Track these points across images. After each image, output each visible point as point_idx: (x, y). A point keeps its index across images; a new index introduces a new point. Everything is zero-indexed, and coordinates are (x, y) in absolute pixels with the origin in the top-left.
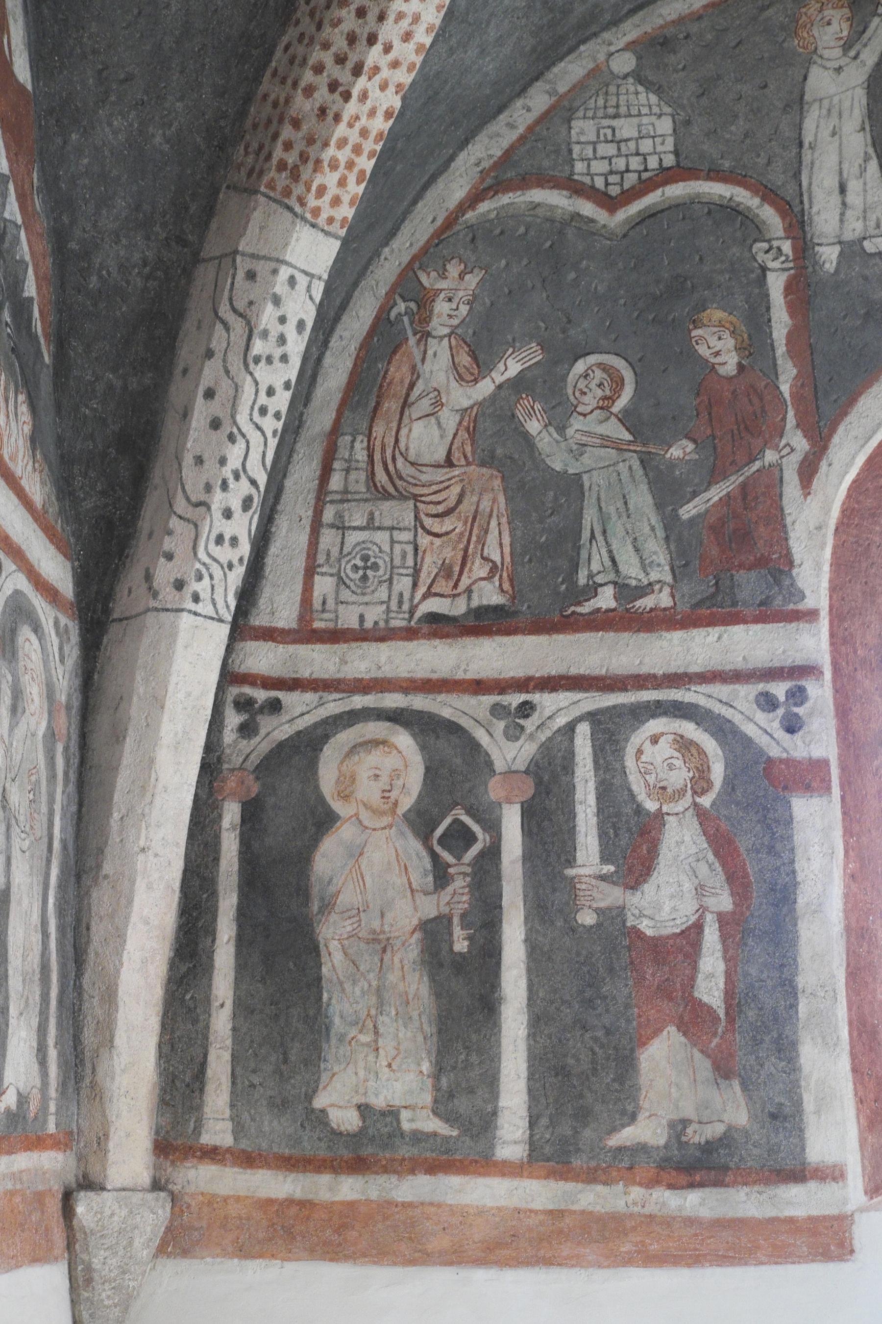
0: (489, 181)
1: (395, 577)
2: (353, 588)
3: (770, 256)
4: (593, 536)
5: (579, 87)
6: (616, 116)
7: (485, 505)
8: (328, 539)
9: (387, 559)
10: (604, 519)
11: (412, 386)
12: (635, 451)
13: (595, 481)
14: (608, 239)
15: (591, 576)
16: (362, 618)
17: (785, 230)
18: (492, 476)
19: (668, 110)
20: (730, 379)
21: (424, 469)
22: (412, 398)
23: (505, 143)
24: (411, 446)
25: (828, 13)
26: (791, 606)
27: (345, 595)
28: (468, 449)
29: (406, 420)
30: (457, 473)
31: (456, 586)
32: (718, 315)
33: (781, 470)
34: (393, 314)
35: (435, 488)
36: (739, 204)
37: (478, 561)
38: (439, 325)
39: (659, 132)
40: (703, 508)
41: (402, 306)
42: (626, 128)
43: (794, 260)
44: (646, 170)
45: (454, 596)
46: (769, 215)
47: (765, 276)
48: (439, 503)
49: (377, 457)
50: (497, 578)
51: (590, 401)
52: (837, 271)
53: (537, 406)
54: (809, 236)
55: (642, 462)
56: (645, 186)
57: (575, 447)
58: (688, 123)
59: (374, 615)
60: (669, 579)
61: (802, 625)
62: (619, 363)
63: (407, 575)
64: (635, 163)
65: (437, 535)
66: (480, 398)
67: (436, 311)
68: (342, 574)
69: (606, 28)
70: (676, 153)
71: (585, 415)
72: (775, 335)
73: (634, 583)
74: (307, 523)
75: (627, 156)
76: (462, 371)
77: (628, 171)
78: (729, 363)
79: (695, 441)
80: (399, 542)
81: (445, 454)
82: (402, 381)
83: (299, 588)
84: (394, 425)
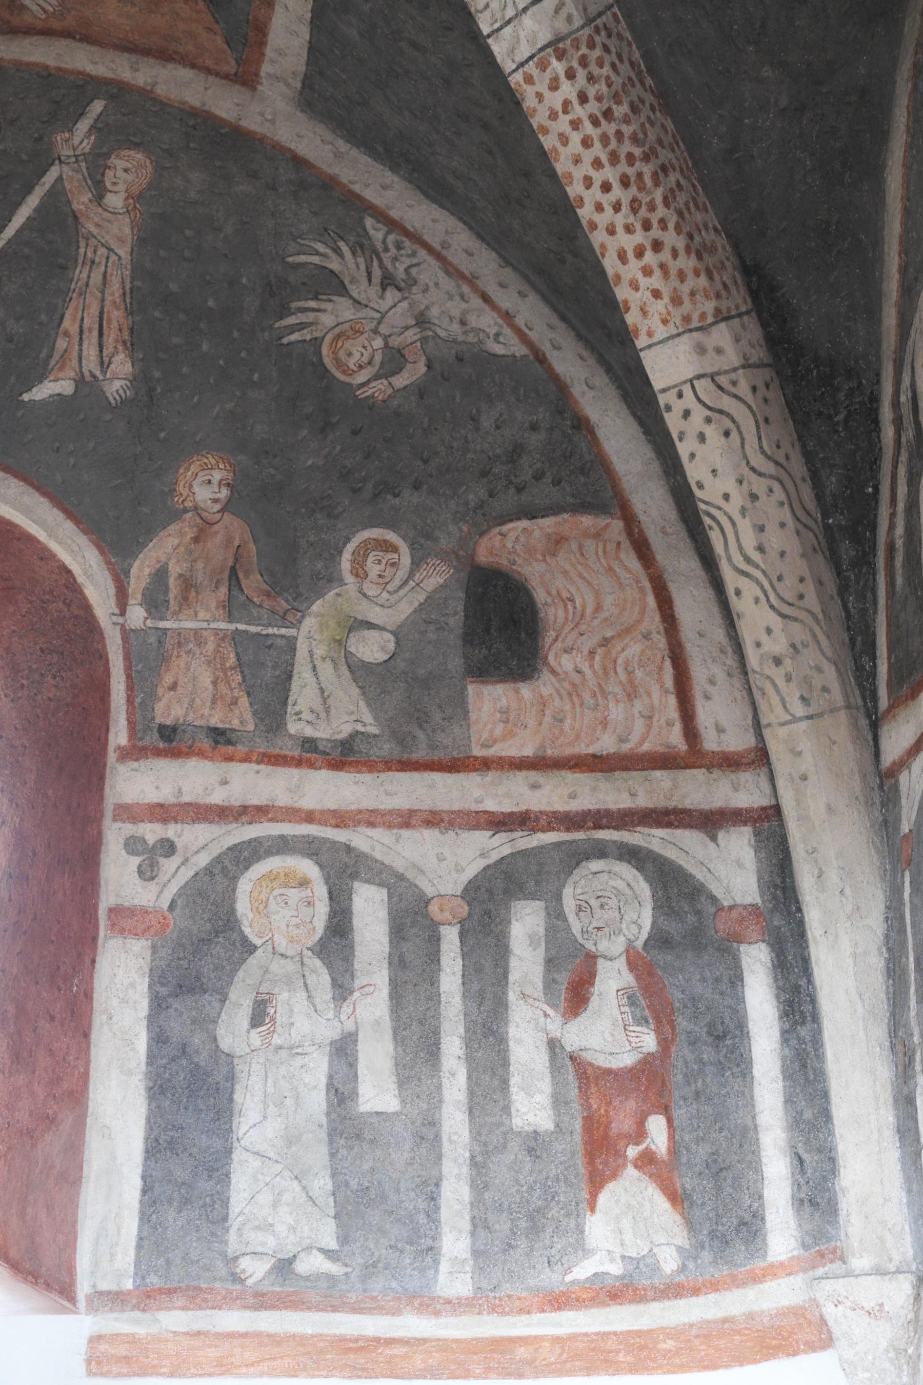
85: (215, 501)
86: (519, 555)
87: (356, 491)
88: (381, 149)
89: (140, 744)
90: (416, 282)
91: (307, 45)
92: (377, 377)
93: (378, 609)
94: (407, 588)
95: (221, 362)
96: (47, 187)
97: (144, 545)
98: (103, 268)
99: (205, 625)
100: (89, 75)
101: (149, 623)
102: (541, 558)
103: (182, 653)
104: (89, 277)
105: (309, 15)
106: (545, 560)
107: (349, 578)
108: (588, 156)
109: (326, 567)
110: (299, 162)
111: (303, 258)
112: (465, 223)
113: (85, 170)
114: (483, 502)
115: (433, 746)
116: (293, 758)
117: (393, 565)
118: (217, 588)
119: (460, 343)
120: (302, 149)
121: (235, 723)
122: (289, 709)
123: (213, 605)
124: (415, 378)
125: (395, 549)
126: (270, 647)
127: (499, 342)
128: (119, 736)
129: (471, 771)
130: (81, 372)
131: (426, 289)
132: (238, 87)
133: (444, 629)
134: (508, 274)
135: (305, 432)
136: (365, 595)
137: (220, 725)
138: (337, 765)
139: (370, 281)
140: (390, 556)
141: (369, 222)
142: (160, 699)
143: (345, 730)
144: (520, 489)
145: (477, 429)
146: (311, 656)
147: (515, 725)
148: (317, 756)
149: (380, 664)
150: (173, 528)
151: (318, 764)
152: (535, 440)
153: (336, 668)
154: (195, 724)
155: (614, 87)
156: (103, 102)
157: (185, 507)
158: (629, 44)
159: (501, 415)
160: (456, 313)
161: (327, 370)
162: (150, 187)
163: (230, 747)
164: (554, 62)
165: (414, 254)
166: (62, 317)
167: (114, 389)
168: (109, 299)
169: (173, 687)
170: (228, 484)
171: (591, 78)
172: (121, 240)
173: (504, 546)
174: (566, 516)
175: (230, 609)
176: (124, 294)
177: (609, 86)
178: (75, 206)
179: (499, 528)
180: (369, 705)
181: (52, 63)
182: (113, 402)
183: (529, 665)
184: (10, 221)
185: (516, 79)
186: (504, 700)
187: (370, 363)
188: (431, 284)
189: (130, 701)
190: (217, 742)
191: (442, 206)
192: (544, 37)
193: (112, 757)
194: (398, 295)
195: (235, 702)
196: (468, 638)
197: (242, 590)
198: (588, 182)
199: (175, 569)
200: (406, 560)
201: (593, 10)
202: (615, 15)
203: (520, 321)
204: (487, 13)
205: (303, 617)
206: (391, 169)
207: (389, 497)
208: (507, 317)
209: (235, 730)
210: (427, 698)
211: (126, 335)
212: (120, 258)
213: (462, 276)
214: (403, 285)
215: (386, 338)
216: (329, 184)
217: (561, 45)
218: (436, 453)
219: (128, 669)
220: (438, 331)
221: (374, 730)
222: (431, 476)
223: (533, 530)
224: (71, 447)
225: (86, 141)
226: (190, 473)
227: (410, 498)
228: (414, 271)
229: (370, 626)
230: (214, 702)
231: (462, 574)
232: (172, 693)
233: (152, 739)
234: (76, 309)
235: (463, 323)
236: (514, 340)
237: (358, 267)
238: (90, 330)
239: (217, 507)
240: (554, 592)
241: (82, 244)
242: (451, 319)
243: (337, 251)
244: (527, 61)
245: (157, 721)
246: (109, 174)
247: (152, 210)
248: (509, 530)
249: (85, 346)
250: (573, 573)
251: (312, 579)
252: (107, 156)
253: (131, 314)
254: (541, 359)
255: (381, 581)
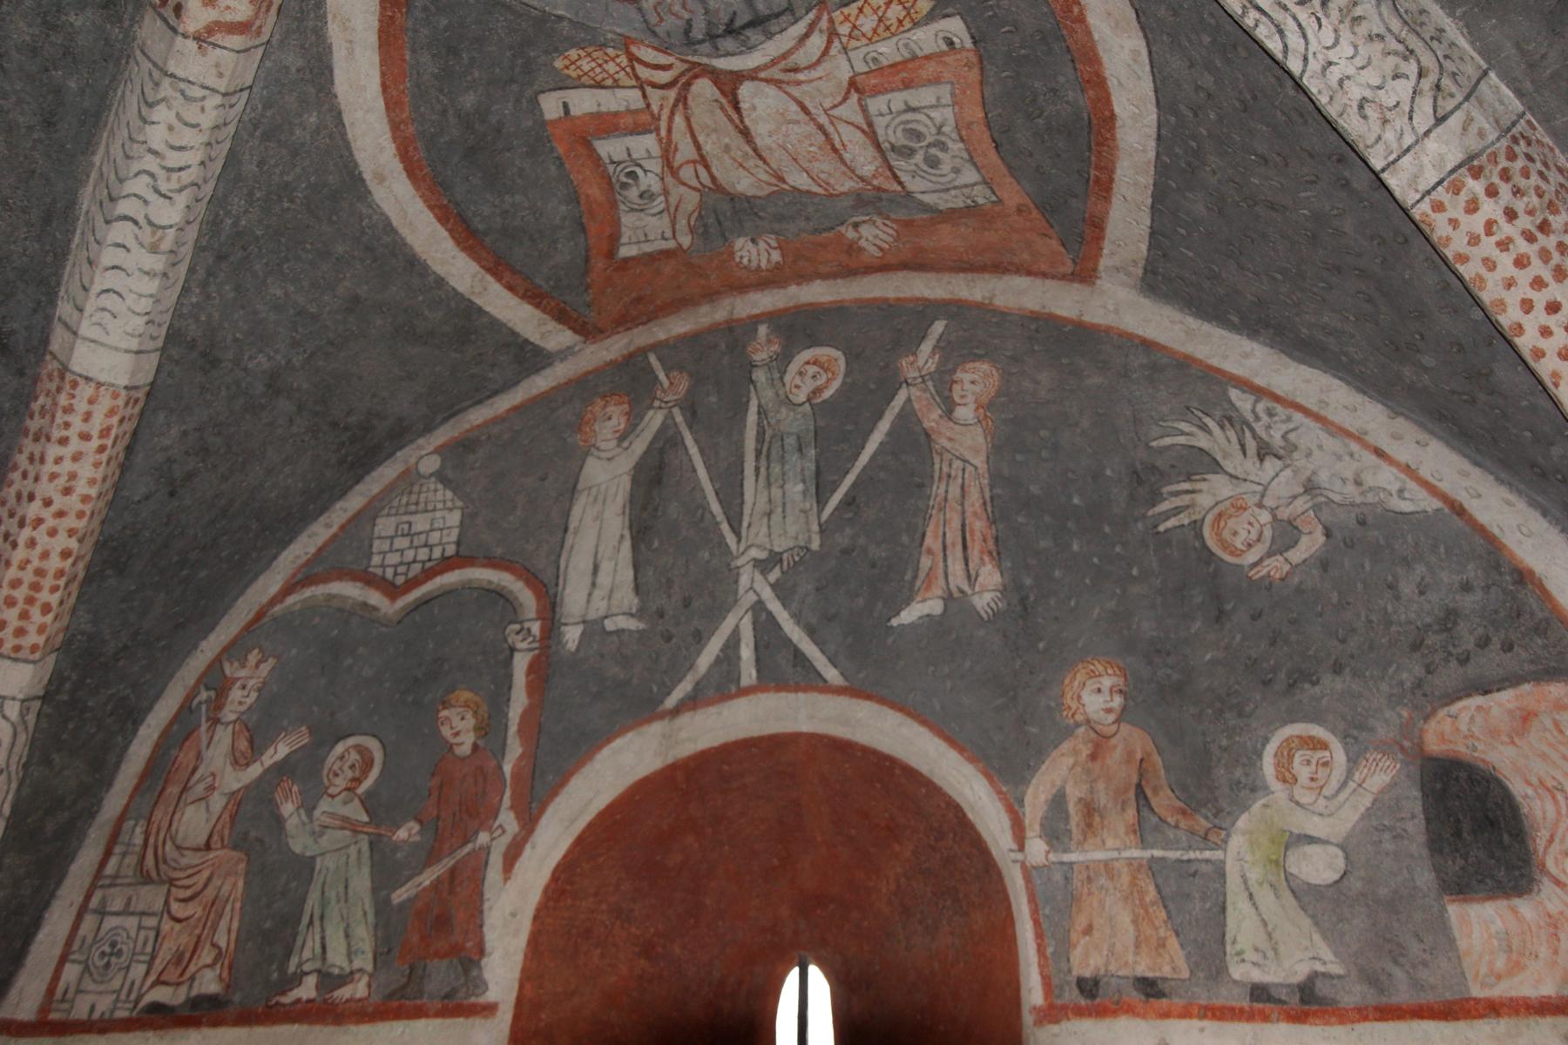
0: (300, 576)
1: (134, 964)
2: (95, 976)
3: (520, 637)
4: (311, 923)
5: (390, 489)
6: (416, 512)
7: (226, 888)
8: (89, 922)
9: (131, 945)
10: (324, 904)
11: (195, 770)
12: (366, 833)
13: (327, 864)
14: (386, 626)
15: (300, 965)
16: (93, 1008)
17: (538, 612)
18: (240, 860)
19: (460, 504)
20: (463, 759)
21: (186, 852)
22: (192, 782)
23: (320, 541)
24: (182, 829)
25: (611, 409)
26: (473, 1000)
27: (88, 984)
28: (226, 832)
29: (181, 804)
30: (211, 856)
31: (182, 975)
32: (466, 695)
33: (488, 853)
34: (195, 703)
35: (190, 871)
36: (504, 588)
37: (208, 946)
38: (229, 714)
39: (448, 525)
40: (414, 892)
41: (204, 695)
42: (420, 523)
43: (542, 639)
44: (430, 560)
45: (178, 984)
46: (527, 598)
47: (512, 656)
48: (188, 887)
49: (152, 840)
50: (219, 966)
51: (341, 783)
52: (578, 649)
53: (295, 789)
54: (557, 617)
55: (371, 843)
56: (429, 574)
57: (317, 829)
58: (473, 516)
59: (104, 1005)
60: (369, 967)
61: (477, 1021)
62: (373, 745)
63: (143, 962)
64: (423, 554)
65: (178, 921)
66: (248, 781)
67: (230, 699)
68: (90, 962)
69: (421, 434)
70: (458, 543)
71: (333, 797)
72: (511, 714)
73: (336, 971)
74: (74, 910)
75: (417, 548)
76: (238, 755)
77: (414, 561)
78: (465, 744)
79: (420, 822)
80: (145, 928)
81: (205, 836)
82: (187, 766)
83: (48, 975)
84: (171, 809)
85: (1109, 711)
86: (1478, 739)
87: (1267, 683)
88: (1235, 320)
89: (1059, 1002)
90: (1296, 447)
91: (1148, 230)
92: (1270, 554)
93: (1316, 818)
94: (1348, 791)
95: (1095, 560)
96: (897, 410)
97: (1036, 769)
98: (960, 480)
99: (1115, 854)
100: (927, 300)
101: (1052, 857)
102: (1508, 740)
103: (1094, 889)
104: (947, 492)
105: (1150, 201)
106: (1513, 743)
107: (1275, 785)
108: (1524, 277)
109: (1247, 775)
110: (1148, 345)
111: (1168, 441)
112: (1340, 379)
113: (932, 389)
114: (1420, 680)
115: (1416, 985)
116: (1242, 1010)
117: (1326, 764)
118: (1123, 809)
119: (1358, 505)
120: (1150, 333)
121: (1166, 971)
122: (1228, 948)
123: (1122, 831)
124: (1314, 549)
125: (1324, 746)
126: (1194, 875)
127: (1404, 499)
128: (1033, 993)
129: (1474, 1017)
130: (948, 588)
131: (1309, 455)
132: (1076, 285)
133: (1402, 837)
134: (1401, 424)
135: (1198, 624)
136: (1298, 803)
137: (1149, 974)
138: (1298, 1017)
139: (1245, 454)
140: (1320, 754)
141: (1234, 394)
142: (1075, 946)
143: (1300, 972)
144: (1464, 660)
145: (1397, 598)
146: (1245, 882)
147: (1522, 954)
148: (1272, 1005)
149: (1330, 886)
150: (1066, 746)
151: (1275, 1016)
152: (1469, 602)
153: (1277, 896)
154: (1120, 973)
155: (1547, 198)
156: (944, 322)
157: (1076, 722)
158: (1552, 150)
159: (1423, 579)
160: (1349, 474)
161: (1213, 554)
162: (998, 394)
163: (1164, 1000)
164: (1470, 182)
165: (1289, 419)
166: (924, 535)
167: (985, 602)
168: (969, 510)
169: (1089, 930)
170: (1121, 691)
171: (1517, 192)
172: (977, 451)
173: (1457, 729)
174: (1527, 687)
175: (1141, 832)
176: (985, 504)
177: (1540, 196)
178: (926, 425)
179: (1446, 709)
180: (1325, 938)
181: (891, 294)
182: (985, 616)
183: (1522, 875)
184: (863, 448)
185: (1421, 211)
186: (1499, 922)
187: (1259, 540)
188: (1314, 448)
189: (1041, 950)
190: (1148, 995)
191: (1311, 366)
192: (1454, 157)
193: (1028, 1019)
194: (1279, 463)
195: (1162, 944)
196: (1435, 844)
197: (1152, 810)
198: (1527, 306)
199: (1074, 793)
200: (1339, 755)
201: (1506, 122)
202: (1529, 122)
203: (1425, 473)
204: (1380, 147)
205: (1228, 835)
206: (1249, 336)
207: (1307, 686)
208: (1408, 470)
209: (1167, 979)
210: (1396, 925)
211: (991, 545)
212: (976, 468)
213: (1349, 434)
214: (1282, 452)
215: (1273, 511)
216: (1185, 363)
217: (1475, 163)
218: (1354, 630)
219: (1035, 912)
220: (1331, 496)
221: (1335, 969)
222: (1352, 657)
223: (1490, 707)
224: (947, 670)
225: (930, 361)
226: (1076, 683)
227: (1332, 684)
228: (1292, 436)
229: (1311, 840)
230: (1137, 946)
231: (1411, 768)
232: (1087, 938)
233: (1072, 996)
234: (937, 525)
235: (1358, 483)
236: (1422, 494)
237: (1229, 441)
238: (953, 544)
239: (1111, 718)
240: (1535, 781)
241: (937, 459)
242: (1344, 481)
243: (1204, 428)
244: (1434, 188)
245: (1075, 973)
246: (956, 387)
247: (1003, 416)
248: (1460, 710)
249: (950, 561)
250: (1555, 756)
251: (1232, 789)
252: (954, 371)
253: (994, 522)
254: (1459, 510)
255: (1314, 784)
